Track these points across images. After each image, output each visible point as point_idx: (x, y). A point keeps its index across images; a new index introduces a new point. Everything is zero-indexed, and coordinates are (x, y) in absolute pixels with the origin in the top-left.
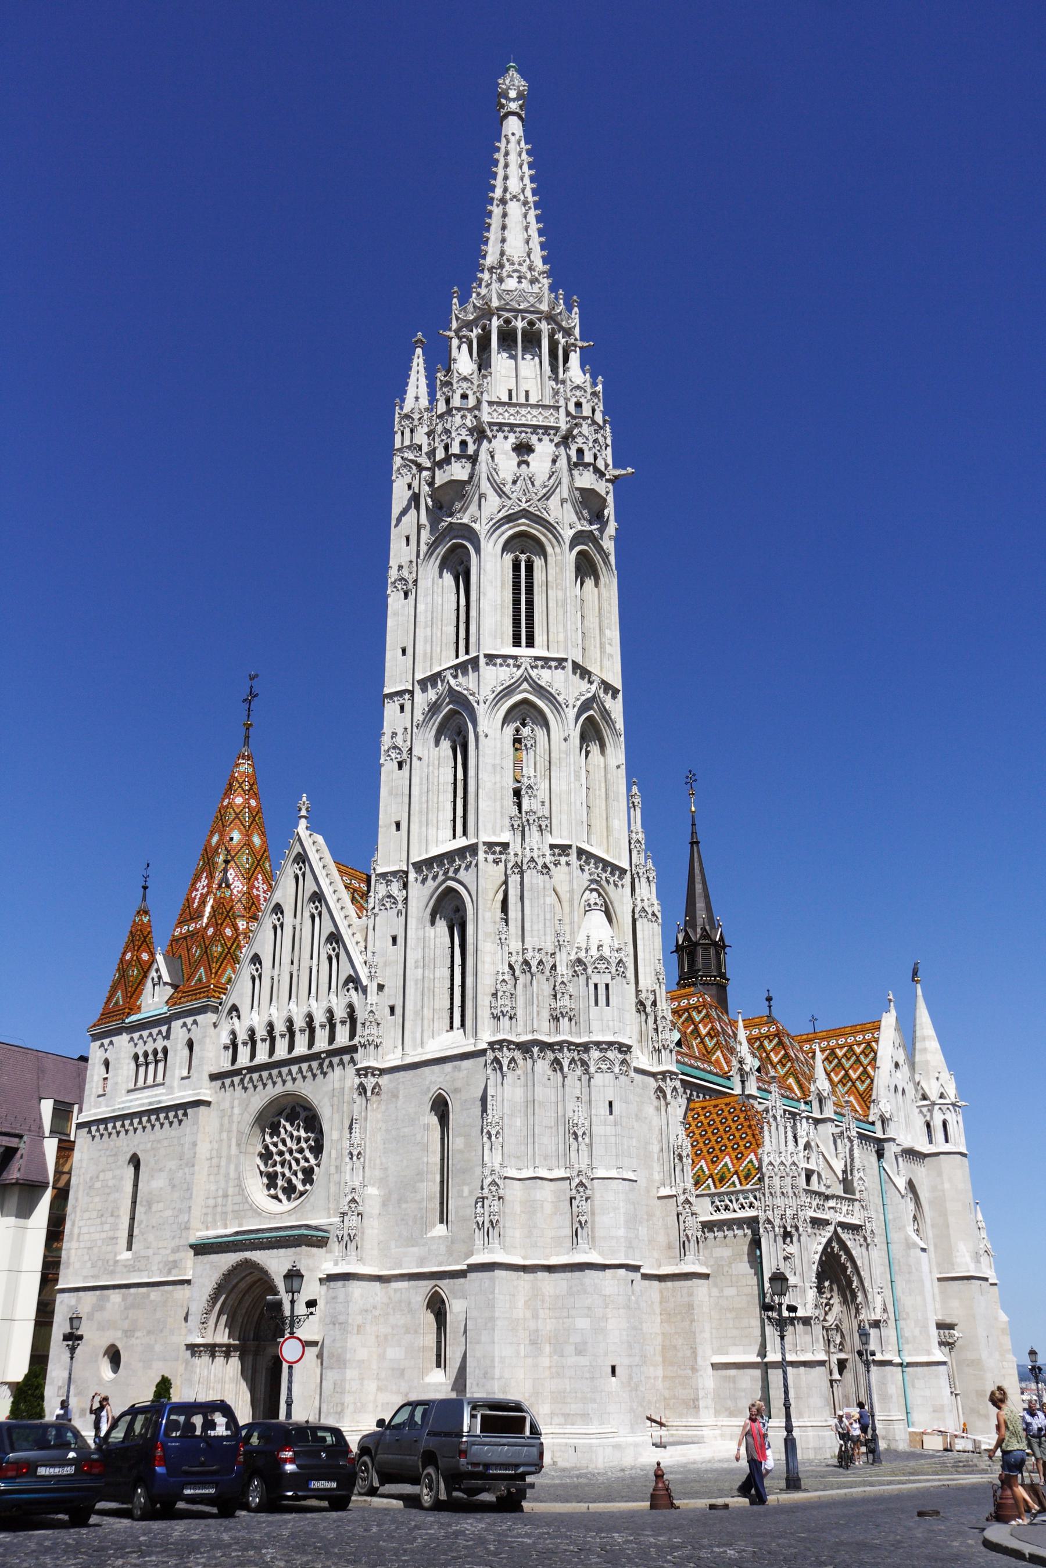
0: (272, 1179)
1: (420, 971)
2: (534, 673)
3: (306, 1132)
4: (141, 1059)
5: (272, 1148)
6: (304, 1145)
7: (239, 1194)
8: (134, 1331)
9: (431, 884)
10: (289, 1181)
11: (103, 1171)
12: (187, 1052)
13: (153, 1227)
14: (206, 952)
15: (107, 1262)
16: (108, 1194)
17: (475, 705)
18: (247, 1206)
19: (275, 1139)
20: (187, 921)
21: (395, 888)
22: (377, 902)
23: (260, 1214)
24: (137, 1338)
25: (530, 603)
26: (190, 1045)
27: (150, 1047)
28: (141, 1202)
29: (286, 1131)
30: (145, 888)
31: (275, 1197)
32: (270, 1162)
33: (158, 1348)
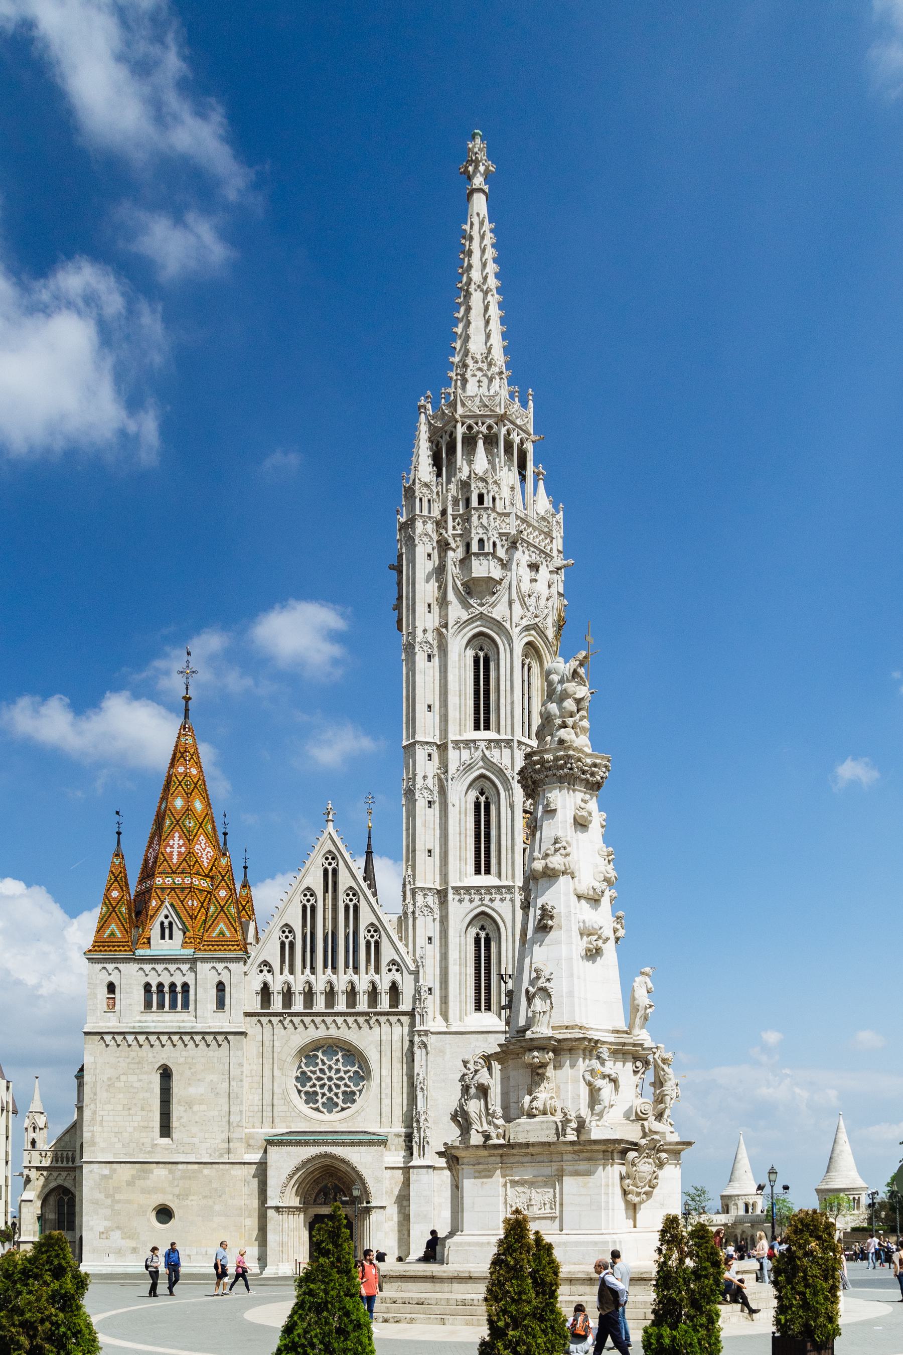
0: (311, 1097)
1: (458, 967)
5: (309, 1074)
6: (342, 1074)
7: (284, 1104)
8: (187, 1195)
9: (466, 903)
11: (124, 1074)
12: (214, 991)
13: (196, 1122)
14: (222, 910)
15: (143, 1144)
16: (136, 1093)
17: (510, 779)
18: (293, 1114)
19: (311, 1068)
20: (169, 873)
21: (432, 900)
23: (309, 1121)
24: (192, 1200)
26: (221, 986)
27: (166, 981)
28: (179, 1103)
29: (324, 1063)
30: (119, 833)
32: (308, 1084)
33: (217, 1208)
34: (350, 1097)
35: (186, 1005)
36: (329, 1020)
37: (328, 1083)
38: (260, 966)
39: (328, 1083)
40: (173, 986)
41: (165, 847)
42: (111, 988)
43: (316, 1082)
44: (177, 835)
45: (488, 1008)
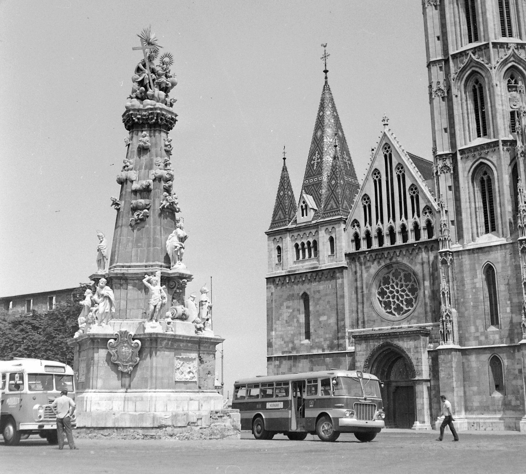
2: (516, 51)
3: (405, 281)
4: (300, 247)
5: (385, 289)
10: (398, 305)
12: (329, 243)
17: (489, 69)
19: (387, 286)
22: (439, 169)
25: (508, 13)
26: (332, 240)
29: (393, 282)
30: (284, 159)
31: (391, 313)
32: (385, 296)
34: (409, 303)
35: (316, 255)
36: (391, 252)
37: (396, 294)
38: (353, 223)
39: (396, 294)
40: (309, 243)
41: (311, 161)
42: (279, 249)
43: (390, 295)
44: (317, 152)
45: (494, 229)
